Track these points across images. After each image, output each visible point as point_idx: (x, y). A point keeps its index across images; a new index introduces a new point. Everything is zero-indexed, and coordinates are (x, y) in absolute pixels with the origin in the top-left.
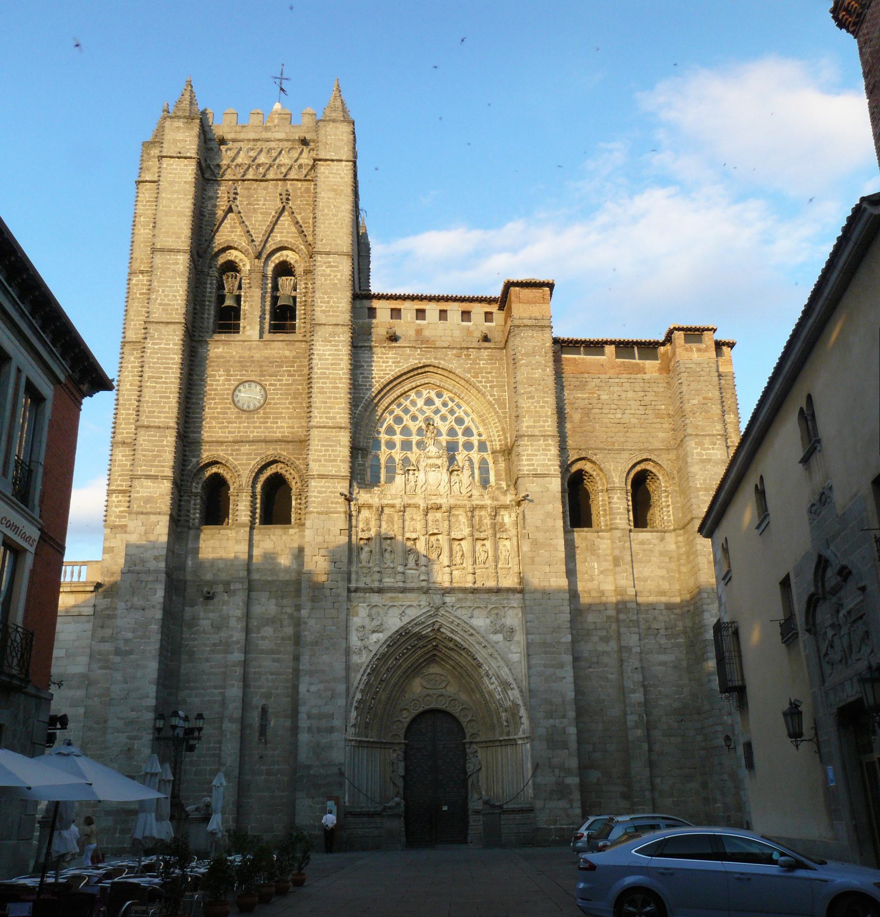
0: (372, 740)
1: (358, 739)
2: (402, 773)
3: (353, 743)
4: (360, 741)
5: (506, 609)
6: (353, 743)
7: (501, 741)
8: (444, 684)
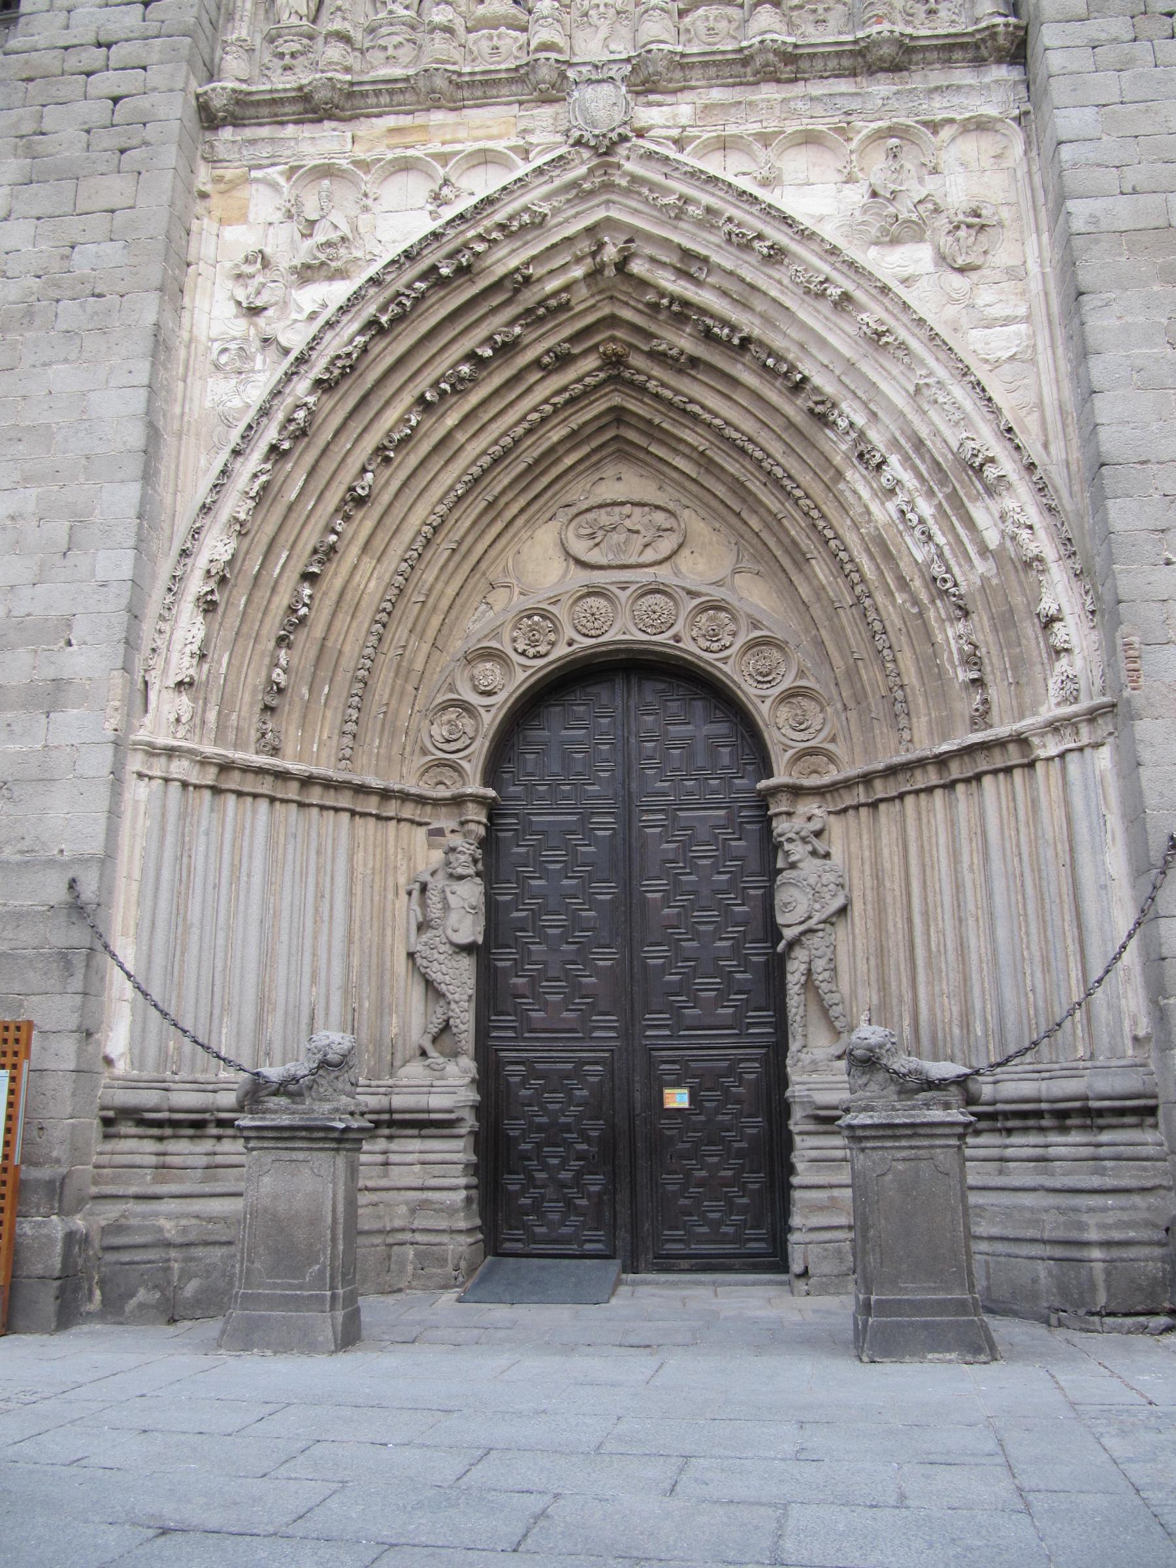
0: (294, 767)
1: (209, 749)
2: (469, 929)
3: (180, 768)
4: (225, 767)
5: (946, 133)
6: (180, 768)
7: (941, 761)
8: (666, 546)
